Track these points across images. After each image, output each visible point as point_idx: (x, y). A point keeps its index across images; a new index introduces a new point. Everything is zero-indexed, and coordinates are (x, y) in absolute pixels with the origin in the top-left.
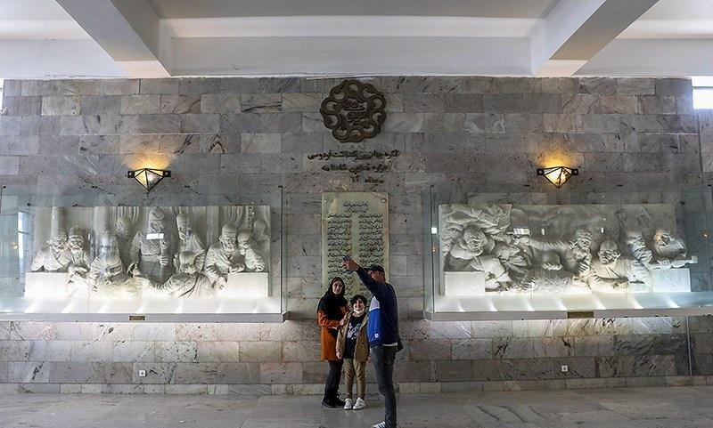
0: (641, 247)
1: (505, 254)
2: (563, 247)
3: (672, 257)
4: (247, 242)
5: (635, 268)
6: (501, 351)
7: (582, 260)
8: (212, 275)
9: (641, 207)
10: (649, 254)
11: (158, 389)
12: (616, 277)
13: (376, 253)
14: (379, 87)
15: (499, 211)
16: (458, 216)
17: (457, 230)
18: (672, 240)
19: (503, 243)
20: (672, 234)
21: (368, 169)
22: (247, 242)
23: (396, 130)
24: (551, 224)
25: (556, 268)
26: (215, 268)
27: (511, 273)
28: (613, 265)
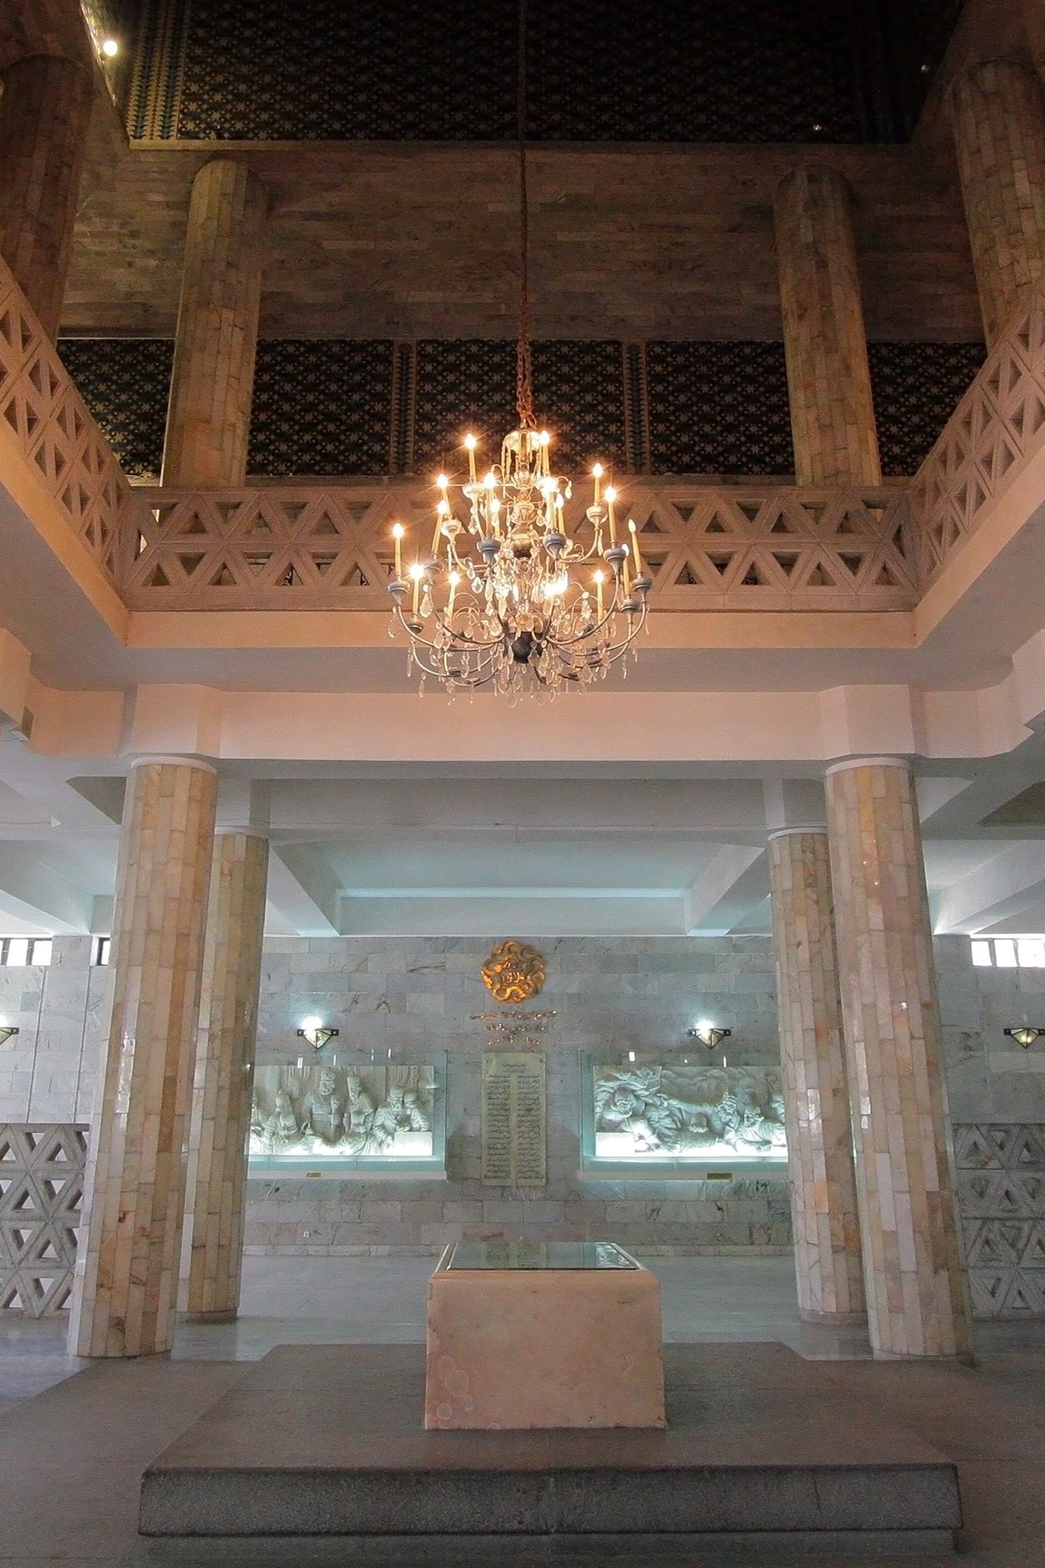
1: (654, 1115)
2: (708, 1109)
4: (414, 1102)
7: (727, 1124)
8: (380, 1134)
11: (321, 1250)
13: (533, 1113)
14: (537, 947)
16: (609, 1078)
19: (654, 1105)
22: (414, 1102)
23: (554, 991)
25: (701, 1130)
26: (383, 1127)
27: (661, 1136)
28: (756, 1128)
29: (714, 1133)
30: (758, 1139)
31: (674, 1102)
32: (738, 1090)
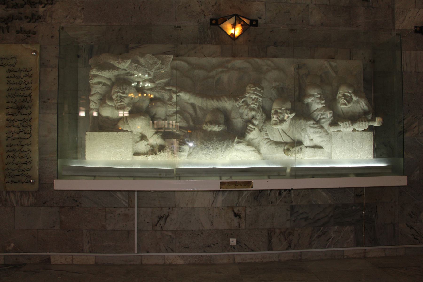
0: (320, 106)
1: (161, 111)
2: (227, 104)
3: (353, 119)
5: (312, 130)
6: (162, 222)
7: (250, 122)
9: (325, 63)
10: (329, 115)
12: (288, 140)
13: (24, 111)
15: (155, 63)
17: (104, 84)
18: (355, 98)
20: (356, 93)
21: (21, 19)
24: (220, 79)
25: (216, 128)
27: (167, 135)
28: (285, 126)
29: (233, 133)
30: (287, 139)
31: (185, 96)
32: (265, 84)
